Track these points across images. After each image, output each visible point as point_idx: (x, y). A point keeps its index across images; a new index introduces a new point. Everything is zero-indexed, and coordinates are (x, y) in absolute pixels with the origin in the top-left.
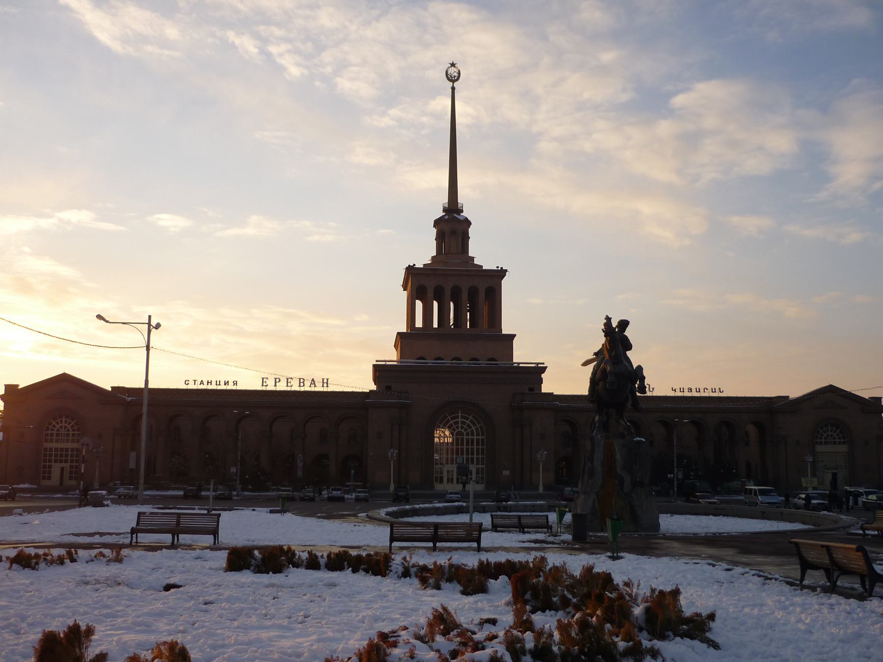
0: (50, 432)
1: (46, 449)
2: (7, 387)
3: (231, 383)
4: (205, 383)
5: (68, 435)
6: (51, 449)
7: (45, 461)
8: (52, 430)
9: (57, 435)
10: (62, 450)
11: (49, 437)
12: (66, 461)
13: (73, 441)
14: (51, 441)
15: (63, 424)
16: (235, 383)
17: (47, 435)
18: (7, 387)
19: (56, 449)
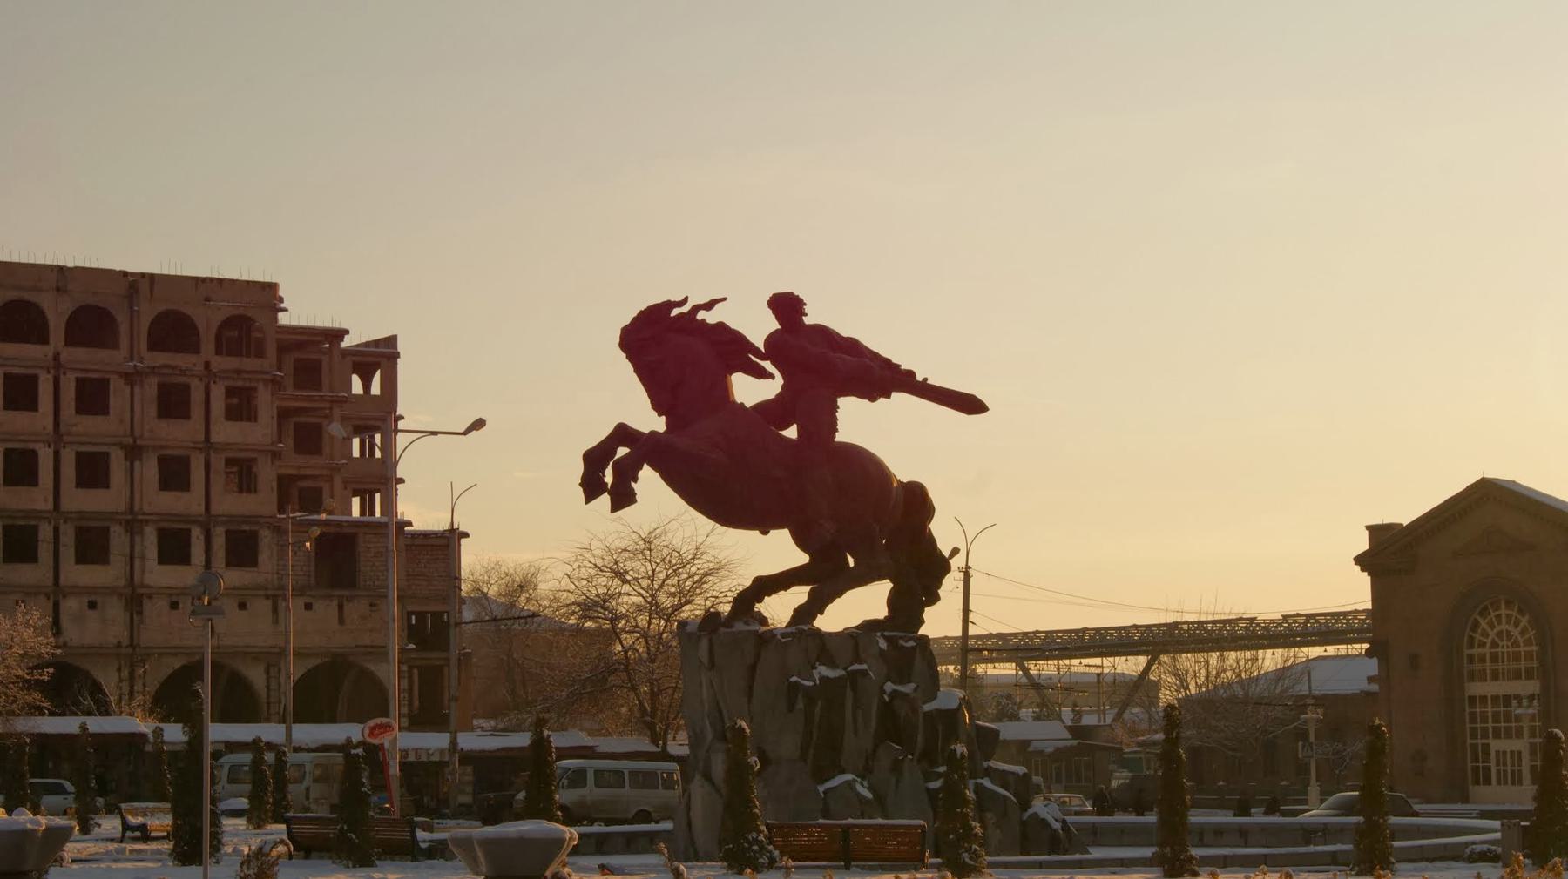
0: (1476, 651)
1: (1472, 699)
2: (1374, 530)
5: (1517, 657)
6: (1484, 699)
7: (1474, 736)
8: (1482, 645)
9: (1495, 658)
10: (1507, 700)
11: (1477, 666)
12: (1519, 735)
13: (1529, 676)
14: (1483, 679)
15: (1504, 627)
17: (1471, 659)
18: (1374, 530)
19: (1495, 699)
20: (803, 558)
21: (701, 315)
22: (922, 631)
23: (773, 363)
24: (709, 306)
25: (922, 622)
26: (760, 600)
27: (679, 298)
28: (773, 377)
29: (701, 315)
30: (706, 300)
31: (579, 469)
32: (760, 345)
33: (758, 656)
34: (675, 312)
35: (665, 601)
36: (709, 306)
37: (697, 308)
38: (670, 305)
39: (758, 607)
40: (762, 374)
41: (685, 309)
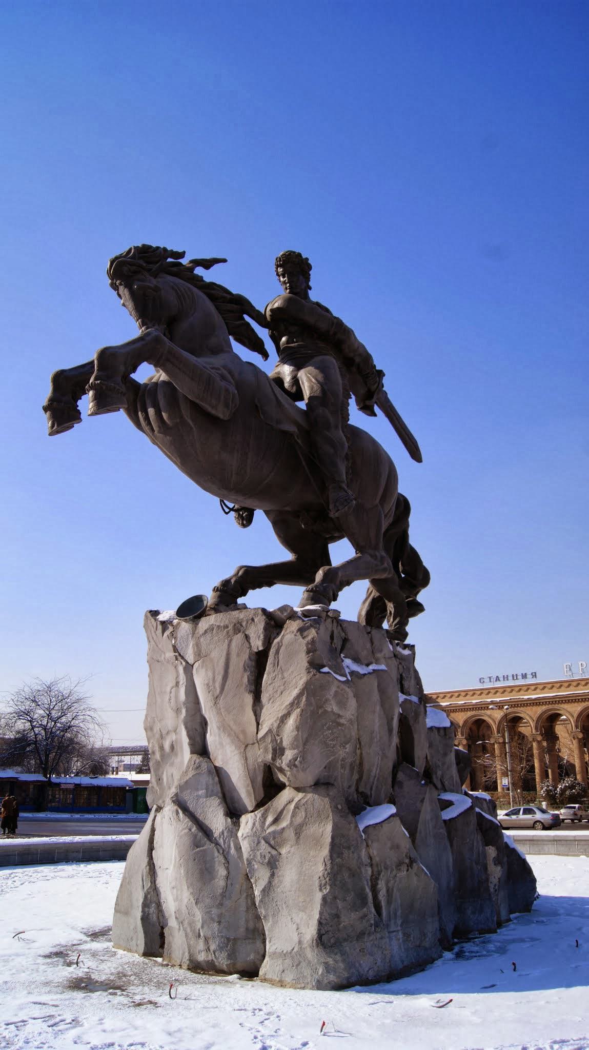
3: (529, 676)
4: (501, 679)
16: (534, 675)
20: (285, 555)
21: (199, 271)
22: (408, 641)
23: (272, 337)
24: (208, 264)
25: (405, 635)
26: (244, 594)
27: (180, 250)
28: (265, 355)
29: (199, 271)
30: (208, 257)
31: (46, 391)
32: (260, 306)
33: (268, 642)
34: (169, 260)
35: (55, 714)
36: (208, 264)
37: (197, 263)
38: (166, 253)
39: (240, 601)
40: (257, 346)
41: (185, 261)
